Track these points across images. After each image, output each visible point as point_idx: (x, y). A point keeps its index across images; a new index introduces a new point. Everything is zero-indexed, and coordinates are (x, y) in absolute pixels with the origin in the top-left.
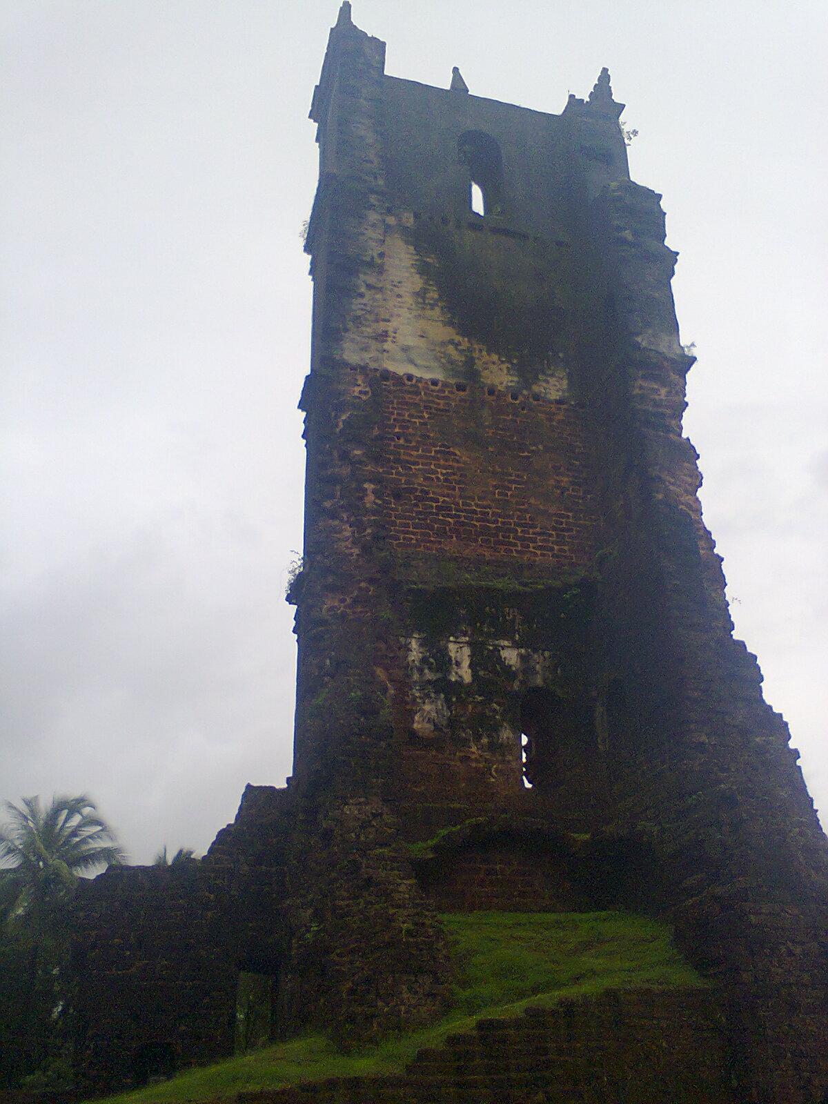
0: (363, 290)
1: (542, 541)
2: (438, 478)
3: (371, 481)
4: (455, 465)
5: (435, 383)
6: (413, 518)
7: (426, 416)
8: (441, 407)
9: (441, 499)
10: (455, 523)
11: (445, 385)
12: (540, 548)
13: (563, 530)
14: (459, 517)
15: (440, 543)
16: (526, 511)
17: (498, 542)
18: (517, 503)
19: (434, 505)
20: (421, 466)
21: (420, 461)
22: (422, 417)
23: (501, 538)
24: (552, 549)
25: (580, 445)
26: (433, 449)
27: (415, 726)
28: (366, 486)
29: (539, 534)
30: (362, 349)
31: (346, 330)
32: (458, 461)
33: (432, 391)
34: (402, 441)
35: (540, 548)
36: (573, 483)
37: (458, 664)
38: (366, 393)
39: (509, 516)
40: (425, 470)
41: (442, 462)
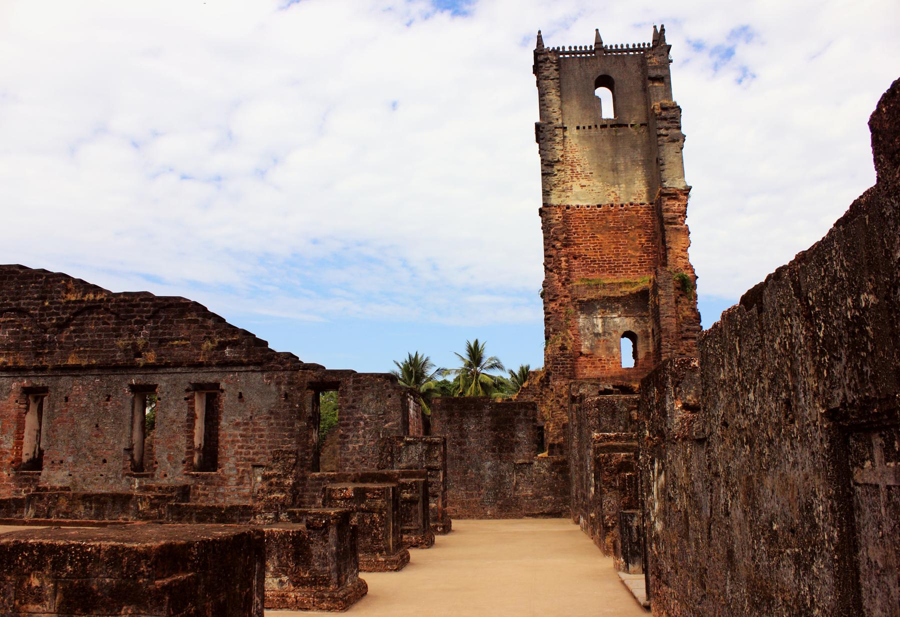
0: (556, 173)
1: (633, 268)
2: (591, 249)
4: (598, 242)
5: (588, 207)
6: (581, 267)
7: (585, 222)
8: (591, 217)
9: (592, 257)
11: (593, 207)
13: (643, 262)
14: (599, 264)
16: (627, 257)
17: (617, 272)
18: (623, 254)
24: (637, 271)
27: (582, 350)
28: (563, 259)
29: (633, 265)
30: (559, 197)
31: (551, 190)
34: (576, 235)
35: (632, 272)
36: (646, 241)
37: (598, 326)
39: (620, 260)
40: (586, 246)
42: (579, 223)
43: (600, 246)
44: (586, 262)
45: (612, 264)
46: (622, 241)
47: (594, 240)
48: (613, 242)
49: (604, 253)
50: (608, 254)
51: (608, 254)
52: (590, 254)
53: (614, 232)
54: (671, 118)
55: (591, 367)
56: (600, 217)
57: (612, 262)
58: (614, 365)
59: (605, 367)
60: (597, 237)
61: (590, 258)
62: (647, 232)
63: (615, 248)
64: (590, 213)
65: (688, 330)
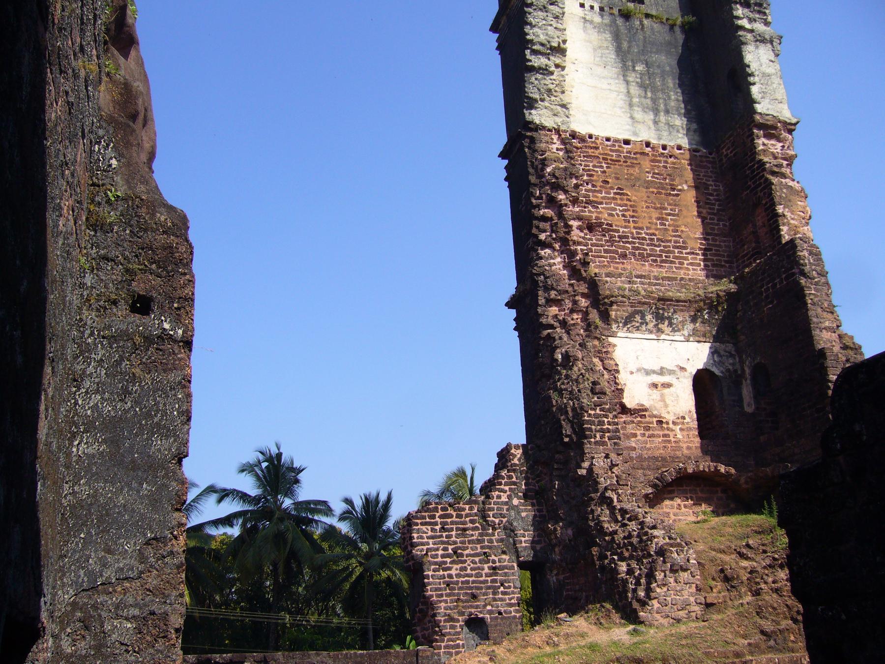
0: (553, 69)
3: (574, 219)
5: (608, 139)
7: (605, 166)
8: (614, 158)
9: (621, 230)
10: (633, 248)
12: (691, 264)
14: (634, 243)
15: (623, 263)
16: (680, 236)
19: (617, 234)
20: (604, 205)
21: (604, 201)
22: (602, 167)
23: (664, 258)
25: (713, 183)
26: (612, 191)
28: (571, 223)
30: (555, 115)
31: (542, 100)
32: (629, 200)
33: (607, 146)
34: (590, 186)
35: (691, 264)
38: (560, 150)
39: (670, 241)
41: (619, 202)
42: (594, 166)
43: (634, 211)
44: (611, 237)
45: (655, 246)
46: (669, 207)
47: (621, 199)
48: (656, 208)
49: (640, 225)
50: (648, 228)
51: (648, 228)
52: (618, 223)
55: (644, 435)
57: (656, 242)
58: (685, 433)
59: (668, 436)
60: (628, 195)
62: (708, 199)
63: (658, 219)
64: (611, 151)
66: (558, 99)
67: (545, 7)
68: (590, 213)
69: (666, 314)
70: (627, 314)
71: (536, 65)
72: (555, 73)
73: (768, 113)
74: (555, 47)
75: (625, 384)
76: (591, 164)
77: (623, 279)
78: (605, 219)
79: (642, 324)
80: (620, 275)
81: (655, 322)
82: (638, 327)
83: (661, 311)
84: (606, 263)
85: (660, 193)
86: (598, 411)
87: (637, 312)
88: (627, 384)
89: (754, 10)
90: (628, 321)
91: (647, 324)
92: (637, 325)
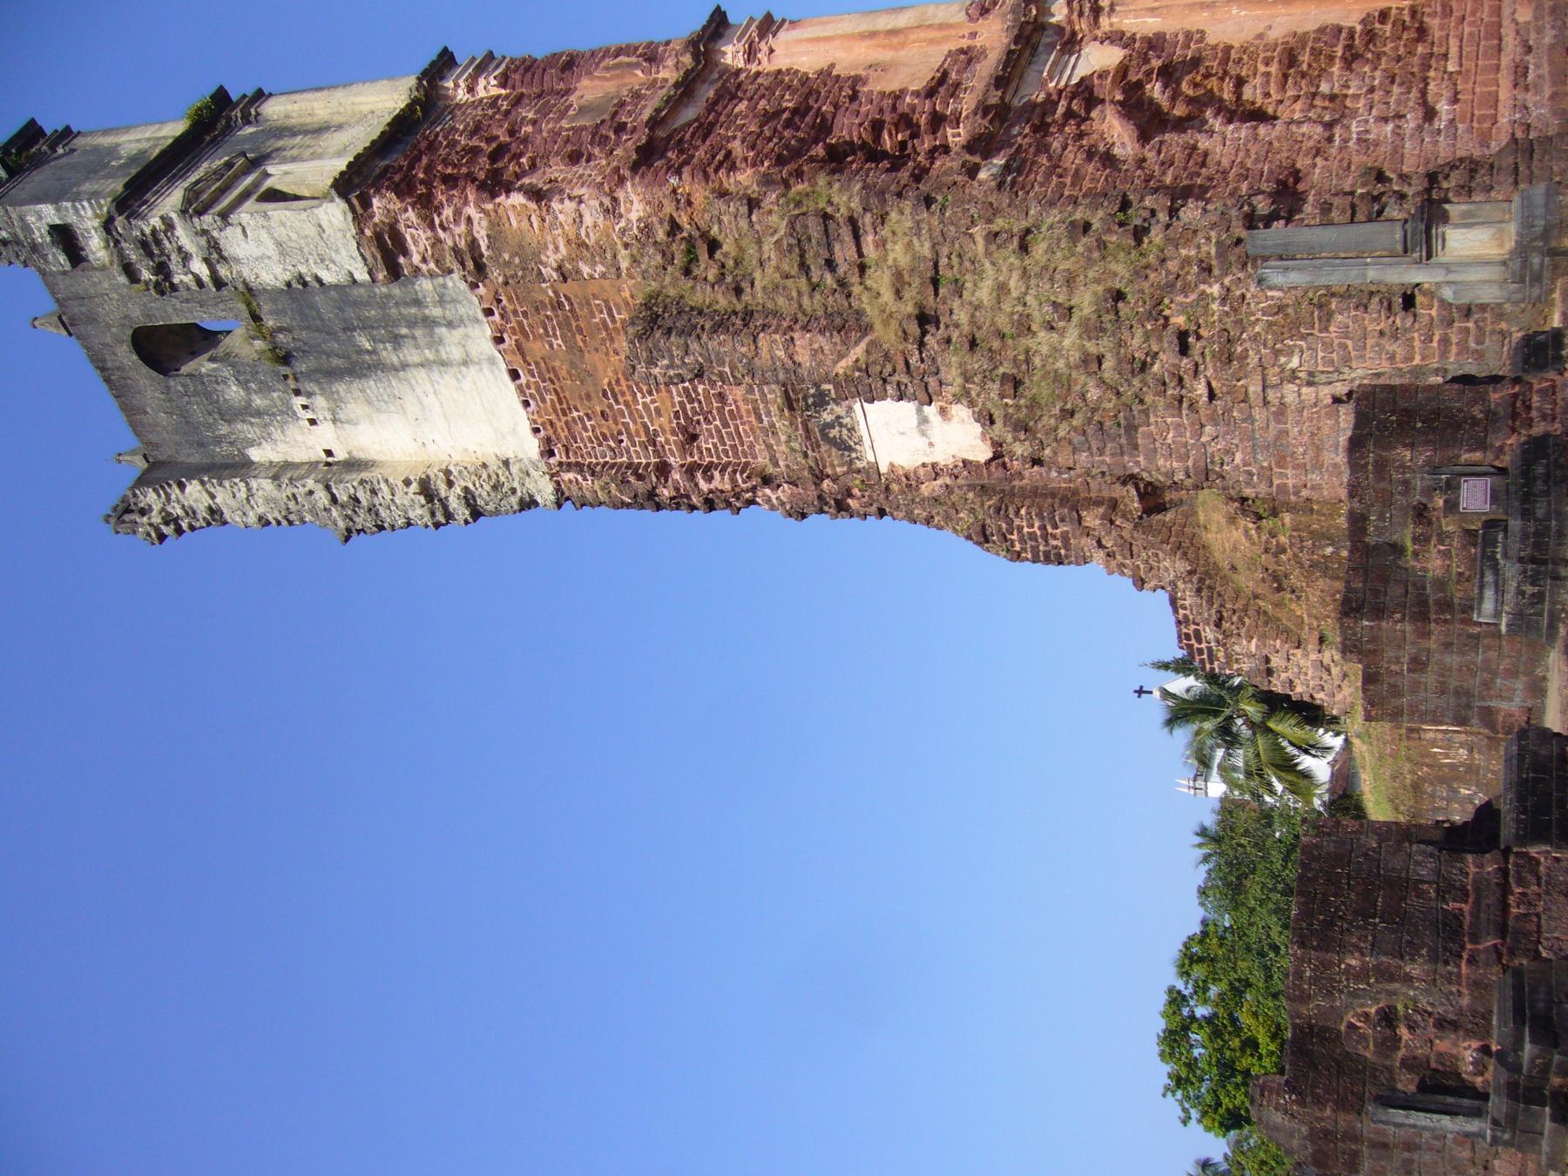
0: (458, 491)
2: (653, 402)
3: (696, 485)
4: (623, 382)
5: (526, 404)
8: (554, 397)
21: (639, 421)
31: (514, 491)
32: (618, 381)
40: (650, 416)
42: (586, 430)
47: (623, 394)
52: (669, 404)
53: (579, 338)
54: (150, 254)
56: (547, 376)
60: (610, 384)
61: (681, 403)
65: (830, 264)
66: (500, 472)
67: (370, 510)
68: (670, 442)
69: (812, 391)
70: (834, 450)
71: (467, 512)
72: (463, 484)
73: (360, 258)
74: (426, 496)
75: (954, 457)
76: (585, 434)
77: (772, 442)
78: (670, 422)
79: (841, 425)
80: (769, 447)
81: (832, 406)
82: (849, 430)
83: (810, 401)
84: (747, 427)
85: (580, 330)
86: (1015, 537)
87: (825, 436)
88: (952, 453)
89: (162, 253)
90: (844, 447)
91: (839, 417)
92: (845, 431)
